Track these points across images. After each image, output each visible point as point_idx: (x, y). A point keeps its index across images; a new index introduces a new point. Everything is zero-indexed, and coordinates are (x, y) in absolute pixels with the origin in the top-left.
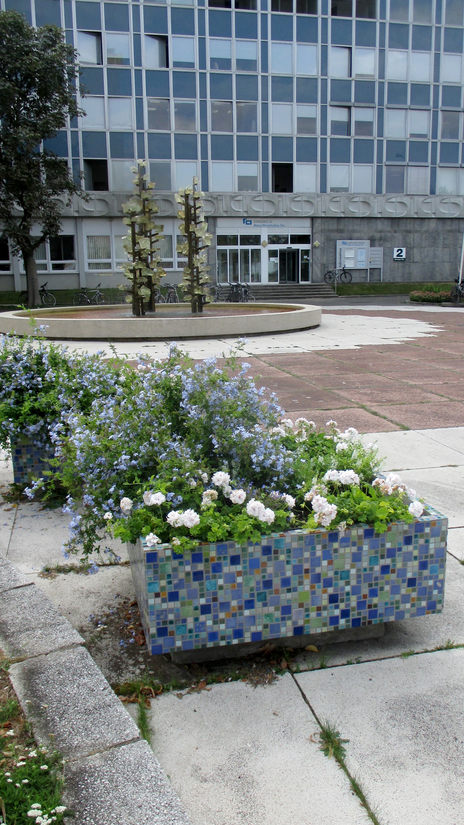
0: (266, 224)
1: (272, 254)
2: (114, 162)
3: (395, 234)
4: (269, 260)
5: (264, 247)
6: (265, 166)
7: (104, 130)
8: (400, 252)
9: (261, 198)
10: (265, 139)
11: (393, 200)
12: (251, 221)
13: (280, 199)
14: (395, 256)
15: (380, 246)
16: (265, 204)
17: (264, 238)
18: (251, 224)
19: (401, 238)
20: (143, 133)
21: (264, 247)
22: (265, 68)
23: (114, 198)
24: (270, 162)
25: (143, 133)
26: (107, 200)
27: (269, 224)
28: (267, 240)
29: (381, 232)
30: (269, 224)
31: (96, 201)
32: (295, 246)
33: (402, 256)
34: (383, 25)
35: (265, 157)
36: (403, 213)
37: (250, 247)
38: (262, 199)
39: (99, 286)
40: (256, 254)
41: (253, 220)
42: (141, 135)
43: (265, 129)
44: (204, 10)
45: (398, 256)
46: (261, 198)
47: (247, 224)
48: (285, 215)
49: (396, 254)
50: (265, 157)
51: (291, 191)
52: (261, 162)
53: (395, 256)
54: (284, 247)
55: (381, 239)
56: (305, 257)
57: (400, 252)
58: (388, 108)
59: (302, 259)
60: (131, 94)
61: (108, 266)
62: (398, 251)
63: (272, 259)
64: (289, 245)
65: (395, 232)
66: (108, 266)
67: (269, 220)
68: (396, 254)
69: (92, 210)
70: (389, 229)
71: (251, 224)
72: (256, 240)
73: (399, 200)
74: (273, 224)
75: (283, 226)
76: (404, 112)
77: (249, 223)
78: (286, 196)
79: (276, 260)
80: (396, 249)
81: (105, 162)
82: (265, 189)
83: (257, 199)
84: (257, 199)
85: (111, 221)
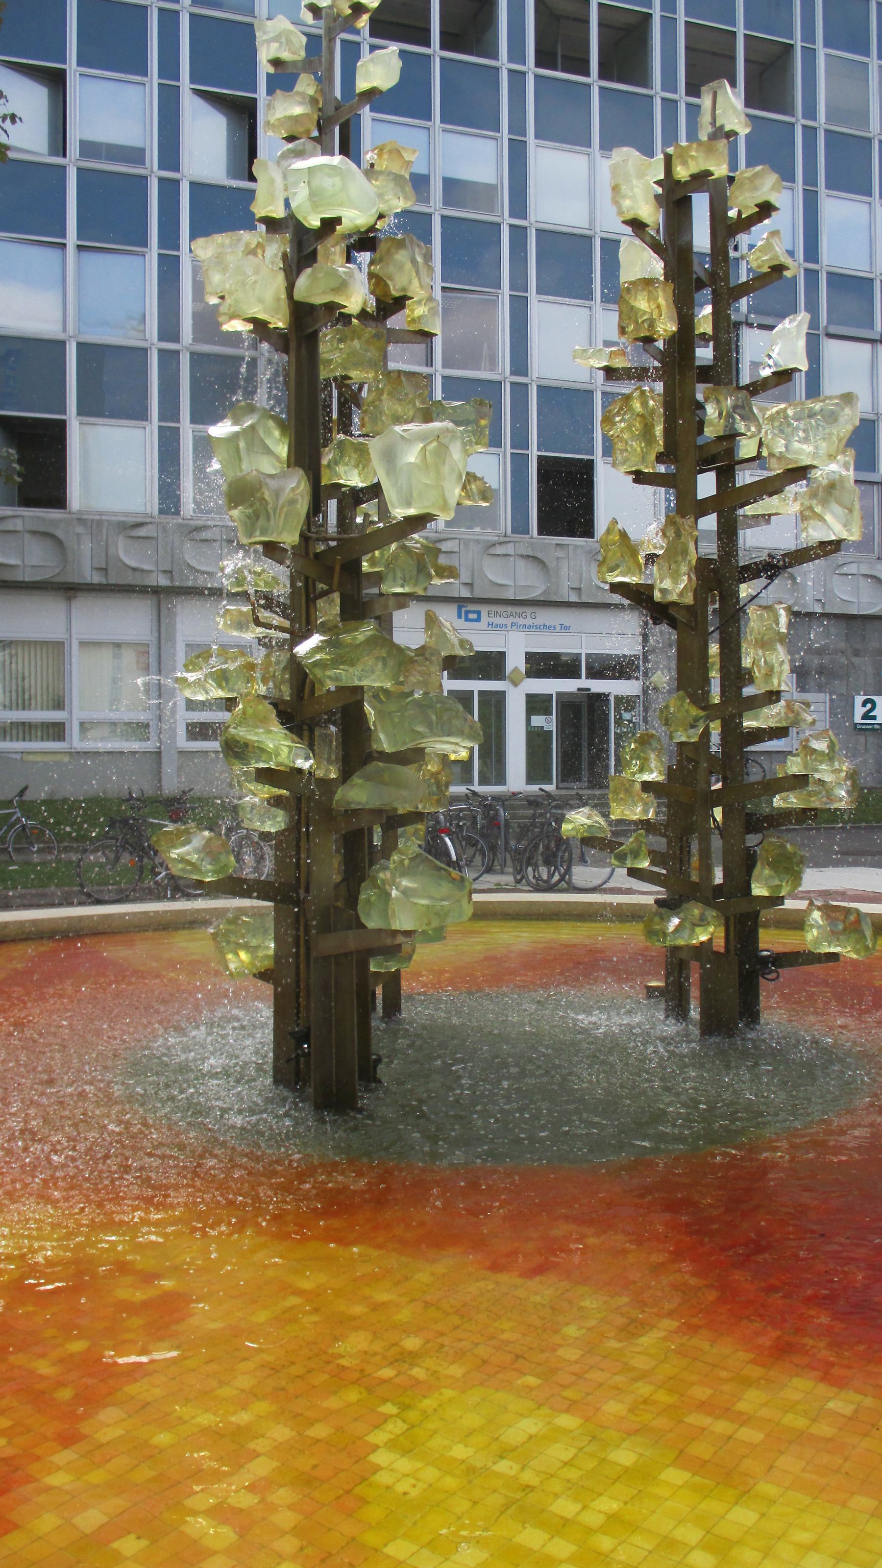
0: (521, 621)
1: (536, 704)
2: (87, 428)
3: (856, 661)
4: (528, 721)
5: (515, 684)
6: (519, 463)
7: (61, 336)
8: (869, 706)
9: (509, 549)
10: (520, 391)
11: (852, 569)
12: (479, 613)
13: (560, 554)
14: (858, 719)
15: (820, 689)
16: (521, 564)
17: (515, 662)
18: (478, 620)
19: (870, 669)
20: (177, 352)
21: (515, 684)
22: (519, 206)
23: (80, 529)
24: (534, 453)
25: (177, 352)
26: (60, 533)
27: (529, 621)
28: (522, 667)
29: (819, 652)
30: (529, 621)
31: (27, 536)
32: (598, 686)
33: (874, 718)
34: (810, 133)
35: (520, 440)
36: (875, 605)
37: (476, 686)
38: (511, 552)
39: (22, 793)
40: (494, 704)
41: (484, 610)
42: (169, 359)
43: (520, 364)
44: (358, 44)
45: (865, 716)
46: (509, 549)
47: (467, 619)
48: (574, 598)
49: (859, 711)
50: (520, 440)
51: (588, 531)
52: (509, 451)
53: (858, 719)
54: (569, 686)
55: (821, 670)
56: (626, 716)
57: (869, 706)
58: (830, 336)
59: (619, 722)
60: (144, 243)
61: (57, 731)
62: (864, 705)
63: (538, 721)
64: (584, 682)
65: (857, 653)
66: (57, 731)
67: (529, 610)
68: (859, 711)
69: (12, 562)
70: (842, 645)
71: (478, 620)
72: (491, 664)
73: (865, 569)
74: (539, 621)
75: (565, 628)
76: (867, 347)
77: (474, 616)
78: (576, 547)
79: (547, 722)
80: (859, 700)
81: (61, 427)
82: (520, 527)
83: (499, 550)
84: (499, 550)
85: (69, 599)
